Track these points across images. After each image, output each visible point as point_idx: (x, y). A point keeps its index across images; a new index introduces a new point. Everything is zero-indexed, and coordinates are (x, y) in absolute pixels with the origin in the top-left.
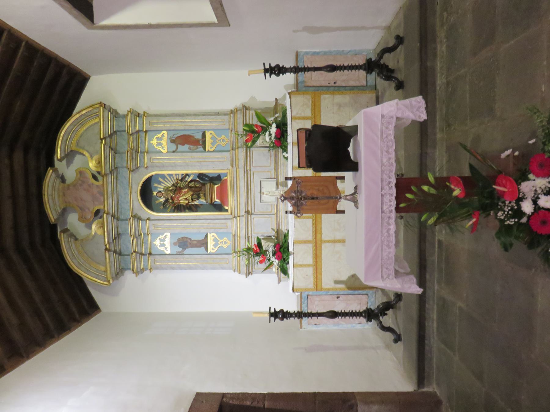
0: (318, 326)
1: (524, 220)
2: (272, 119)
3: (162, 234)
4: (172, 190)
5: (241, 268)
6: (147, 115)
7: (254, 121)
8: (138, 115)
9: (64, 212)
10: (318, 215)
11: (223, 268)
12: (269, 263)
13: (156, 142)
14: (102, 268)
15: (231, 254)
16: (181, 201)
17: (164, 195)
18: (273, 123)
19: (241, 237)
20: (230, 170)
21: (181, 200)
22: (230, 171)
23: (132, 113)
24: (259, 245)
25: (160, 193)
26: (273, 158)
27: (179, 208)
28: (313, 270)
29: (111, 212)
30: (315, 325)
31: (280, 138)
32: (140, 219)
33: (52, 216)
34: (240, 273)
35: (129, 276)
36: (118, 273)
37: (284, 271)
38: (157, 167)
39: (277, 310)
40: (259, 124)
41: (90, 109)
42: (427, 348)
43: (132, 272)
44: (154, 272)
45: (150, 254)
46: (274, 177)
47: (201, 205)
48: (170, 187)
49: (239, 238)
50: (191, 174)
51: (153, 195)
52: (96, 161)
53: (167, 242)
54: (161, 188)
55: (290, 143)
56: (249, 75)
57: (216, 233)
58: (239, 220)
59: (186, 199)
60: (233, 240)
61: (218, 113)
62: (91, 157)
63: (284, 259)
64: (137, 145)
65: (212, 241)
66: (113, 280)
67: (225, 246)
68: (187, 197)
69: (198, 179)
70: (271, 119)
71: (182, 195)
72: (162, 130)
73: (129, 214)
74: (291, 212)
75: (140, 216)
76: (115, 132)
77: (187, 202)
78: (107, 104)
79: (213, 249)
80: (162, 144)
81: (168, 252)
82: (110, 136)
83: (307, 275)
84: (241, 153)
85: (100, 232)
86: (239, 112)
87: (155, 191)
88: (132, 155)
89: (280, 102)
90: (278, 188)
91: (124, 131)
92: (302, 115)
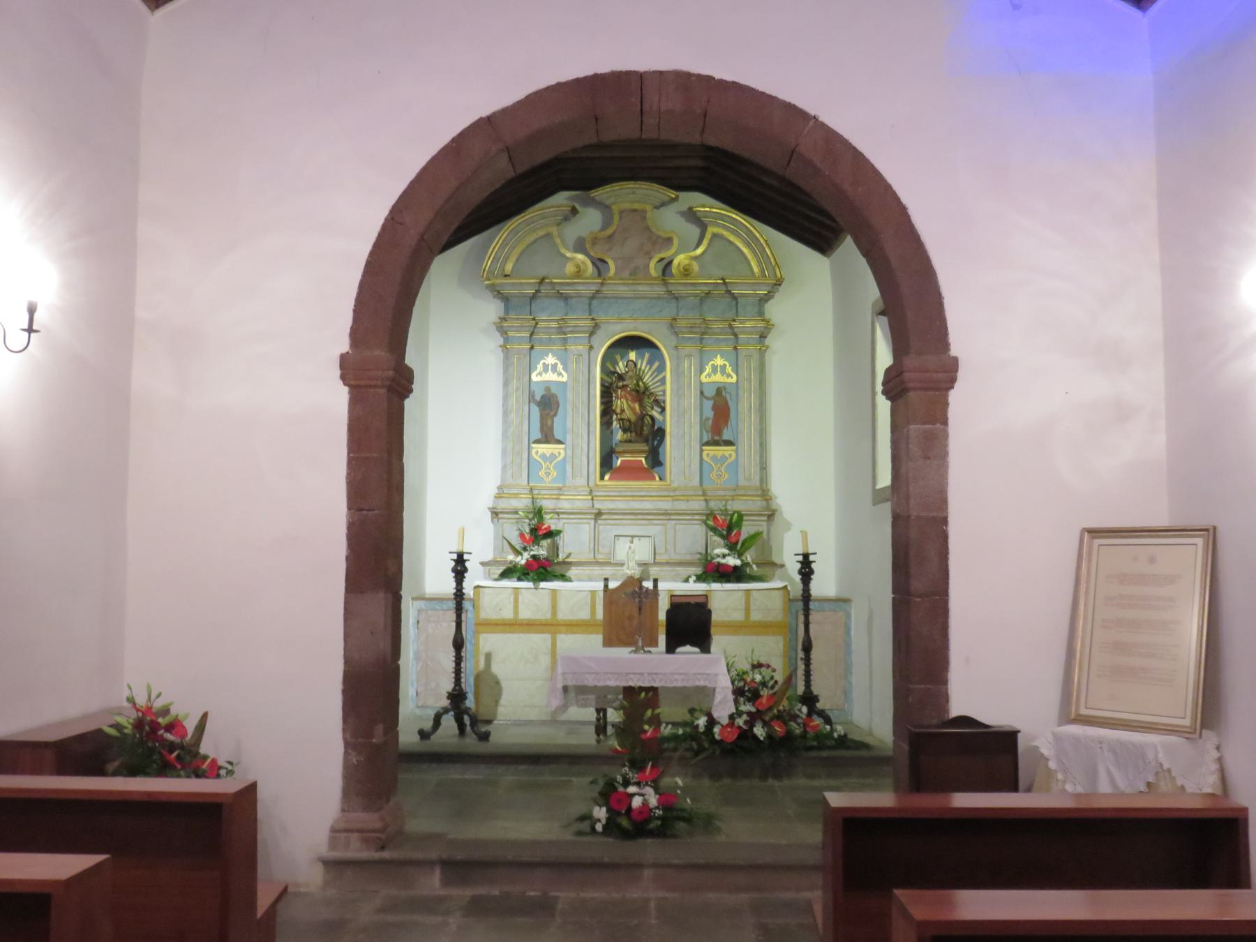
0: (416, 626)
1: (621, 789)
2: (749, 560)
3: (565, 369)
4: (638, 385)
5: (503, 499)
6: (762, 354)
7: (747, 530)
8: (763, 336)
9: (605, 208)
10: (601, 629)
11: (504, 468)
12: (519, 549)
13: (719, 364)
14: (509, 267)
15: (528, 483)
16: (619, 401)
17: (630, 373)
18: (742, 561)
19: (557, 501)
20: (670, 485)
21: (622, 402)
22: (668, 485)
23: (766, 328)
24: (550, 534)
25: (633, 366)
26: (688, 557)
27: (607, 393)
28: (509, 620)
29: (604, 289)
30: (418, 622)
31: (717, 571)
32: (592, 334)
33: (600, 193)
34: (495, 497)
35: (492, 309)
36: (498, 292)
37: (506, 574)
38: (678, 365)
39: (467, 564)
40: (742, 538)
41: (772, 260)
42: (425, 766)
43: (502, 315)
44: (500, 349)
45: (532, 348)
46: (657, 558)
47: (612, 433)
48: (642, 380)
49: (555, 497)
50: (664, 416)
51: (630, 351)
52: (689, 265)
53: (551, 376)
54: (643, 365)
55: (710, 587)
56: (801, 532)
57: (565, 458)
58: (587, 500)
59: (623, 411)
60: (552, 487)
61: (765, 469)
62: (696, 258)
63: (528, 574)
64: (714, 334)
65: (550, 451)
66: (488, 287)
67: (542, 473)
68: (627, 411)
69: (656, 427)
70: (749, 557)
71: (630, 403)
72: (737, 375)
73: (601, 317)
74: (606, 586)
75: (595, 333)
76: (735, 298)
77: (618, 411)
78: (781, 288)
79: (537, 452)
80: (715, 375)
81: (534, 378)
82: (729, 292)
83: (500, 609)
84: (698, 505)
85: (570, 268)
86: (764, 503)
87: (636, 354)
88: (700, 327)
89: (779, 572)
90: (640, 565)
91: (737, 315)
92: (752, 607)
